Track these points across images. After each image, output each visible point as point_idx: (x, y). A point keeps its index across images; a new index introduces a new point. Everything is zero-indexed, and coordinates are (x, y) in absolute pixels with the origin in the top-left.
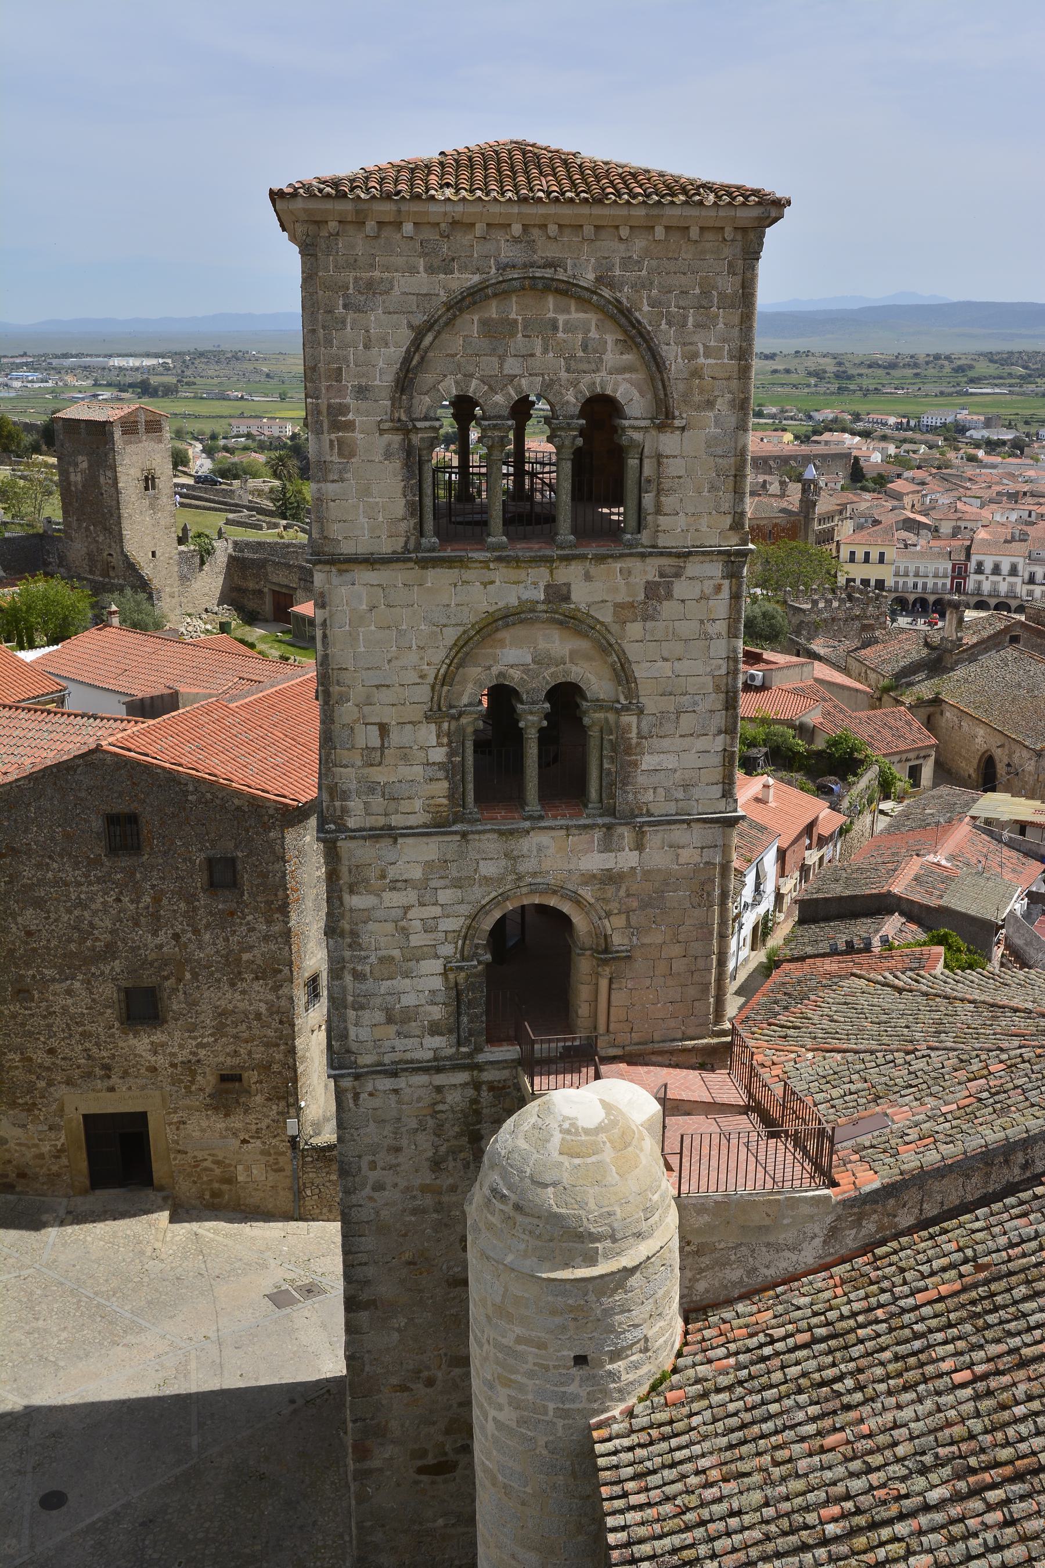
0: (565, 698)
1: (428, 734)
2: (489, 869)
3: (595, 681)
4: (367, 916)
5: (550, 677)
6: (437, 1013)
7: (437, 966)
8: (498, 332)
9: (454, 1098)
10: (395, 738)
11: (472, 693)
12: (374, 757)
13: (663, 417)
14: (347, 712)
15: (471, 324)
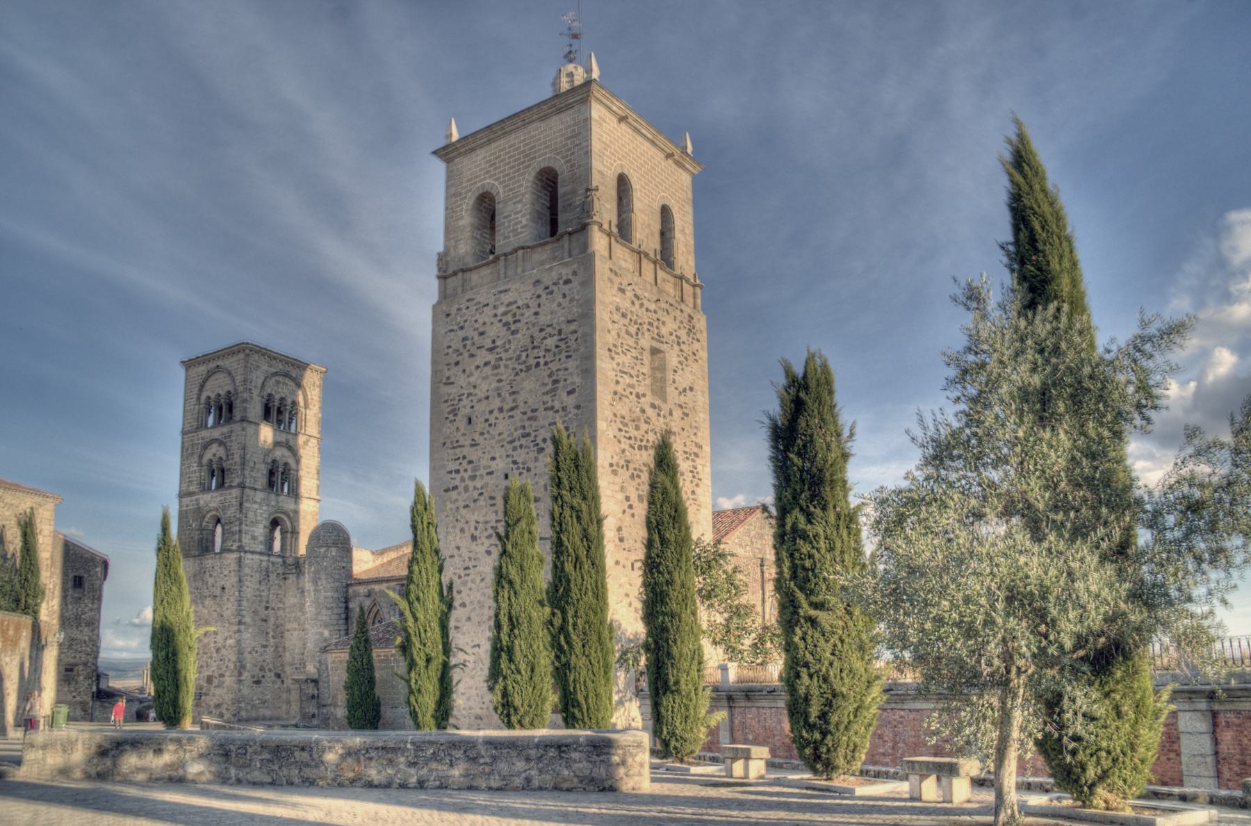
0: (286, 464)
1: (263, 466)
2: (273, 503)
3: (291, 462)
4: (248, 509)
5: (284, 460)
6: (261, 539)
7: (261, 526)
8: (278, 382)
9: (264, 564)
10: (258, 466)
11: (269, 460)
12: (253, 469)
13: (306, 407)
14: (248, 457)
15: (273, 379)
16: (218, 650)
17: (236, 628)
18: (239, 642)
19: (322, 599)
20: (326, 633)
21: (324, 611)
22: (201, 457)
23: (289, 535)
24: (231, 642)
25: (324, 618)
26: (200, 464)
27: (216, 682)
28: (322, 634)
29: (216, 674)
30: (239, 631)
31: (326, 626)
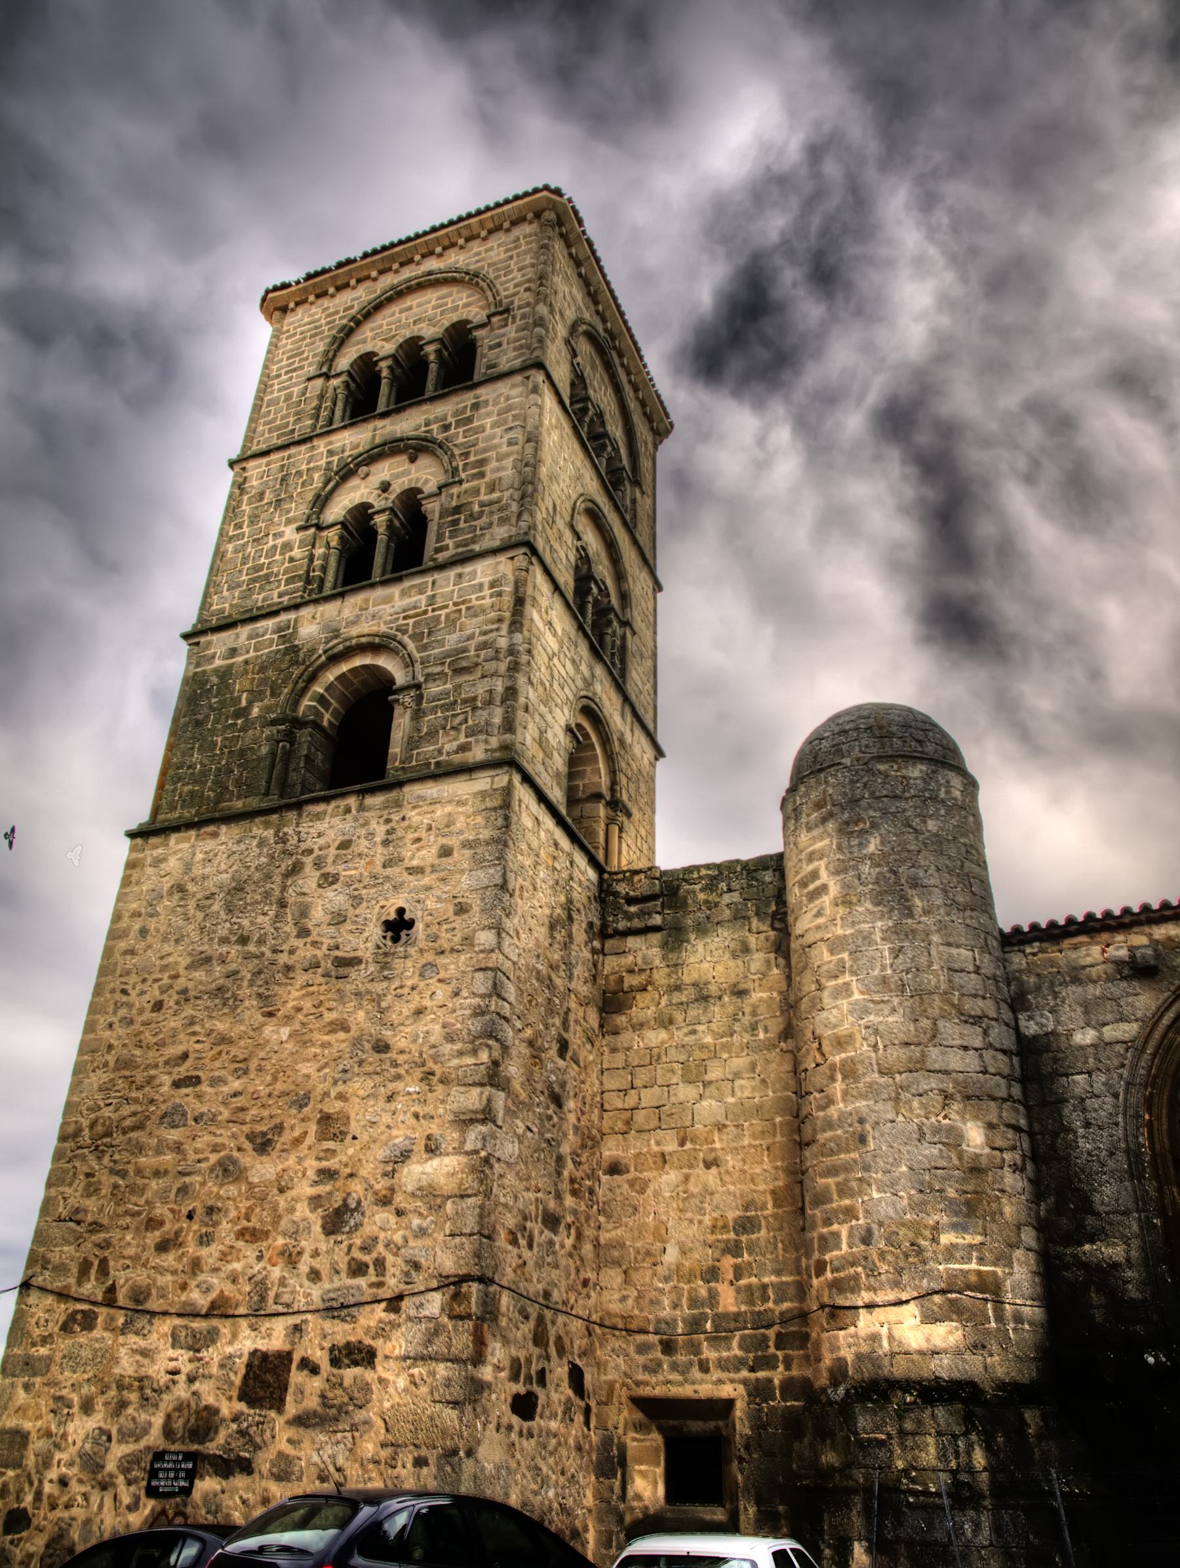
16: (337, 1221)
17: (473, 1099)
18: (483, 1165)
19: (935, 978)
20: (975, 1136)
21: (951, 1031)
22: (321, 501)
23: (602, 811)
24: (442, 1170)
25: (956, 1061)
26: (313, 524)
27: (305, 1391)
28: (953, 1140)
29: (315, 1349)
30: (486, 1115)
31: (972, 1097)
